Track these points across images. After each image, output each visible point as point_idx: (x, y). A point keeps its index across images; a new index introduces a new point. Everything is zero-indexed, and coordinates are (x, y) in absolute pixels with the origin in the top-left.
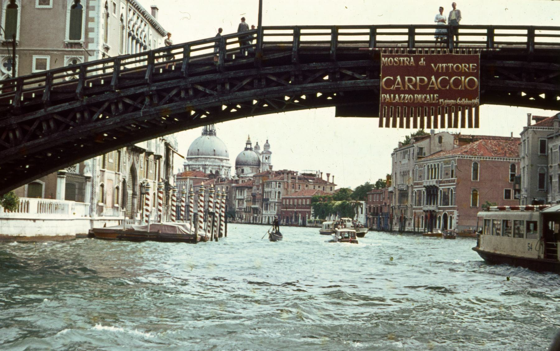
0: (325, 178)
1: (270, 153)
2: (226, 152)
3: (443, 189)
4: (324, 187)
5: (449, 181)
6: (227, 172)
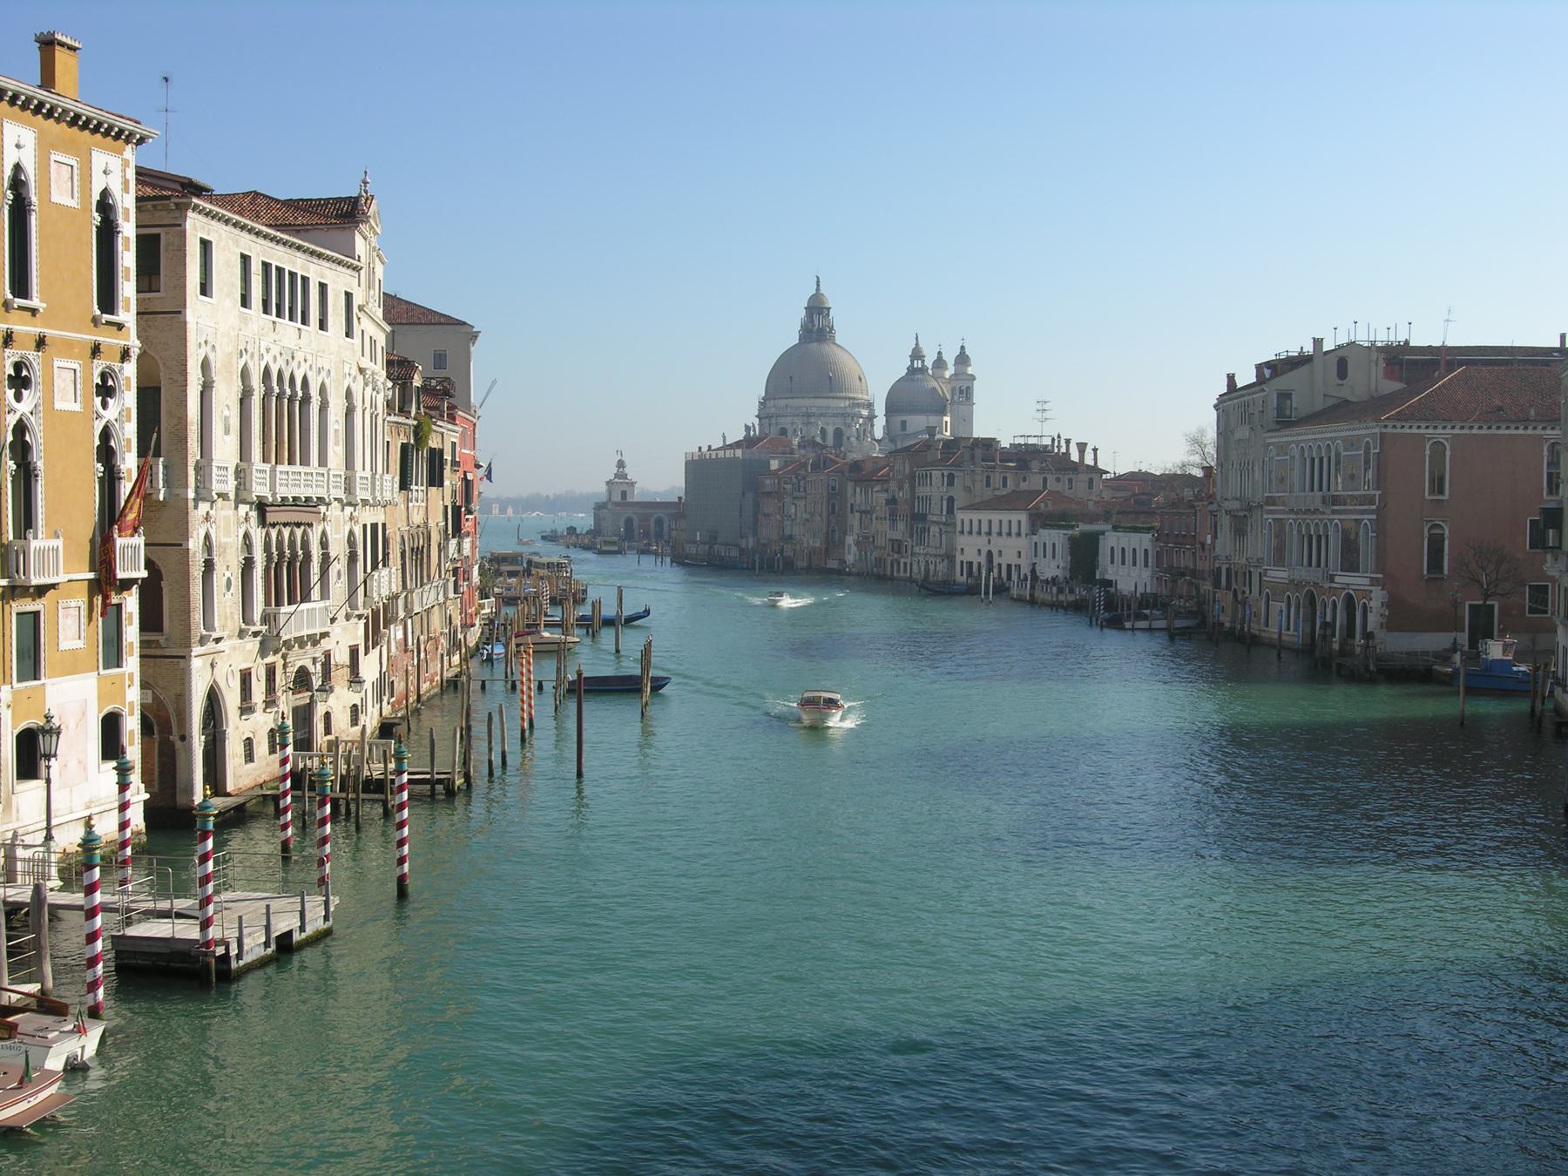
0: (1075, 457)
1: (973, 378)
2: (860, 379)
4: (1070, 481)
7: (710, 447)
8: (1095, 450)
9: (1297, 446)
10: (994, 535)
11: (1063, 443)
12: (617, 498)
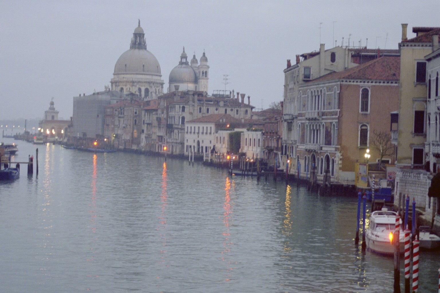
1: (208, 67)
2: (158, 67)
3: (325, 123)
4: (237, 111)
5: (332, 114)
6: (159, 90)
7: (84, 94)
8: (249, 98)
9: (310, 91)
10: (200, 133)
11: (235, 94)
12: (50, 118)
